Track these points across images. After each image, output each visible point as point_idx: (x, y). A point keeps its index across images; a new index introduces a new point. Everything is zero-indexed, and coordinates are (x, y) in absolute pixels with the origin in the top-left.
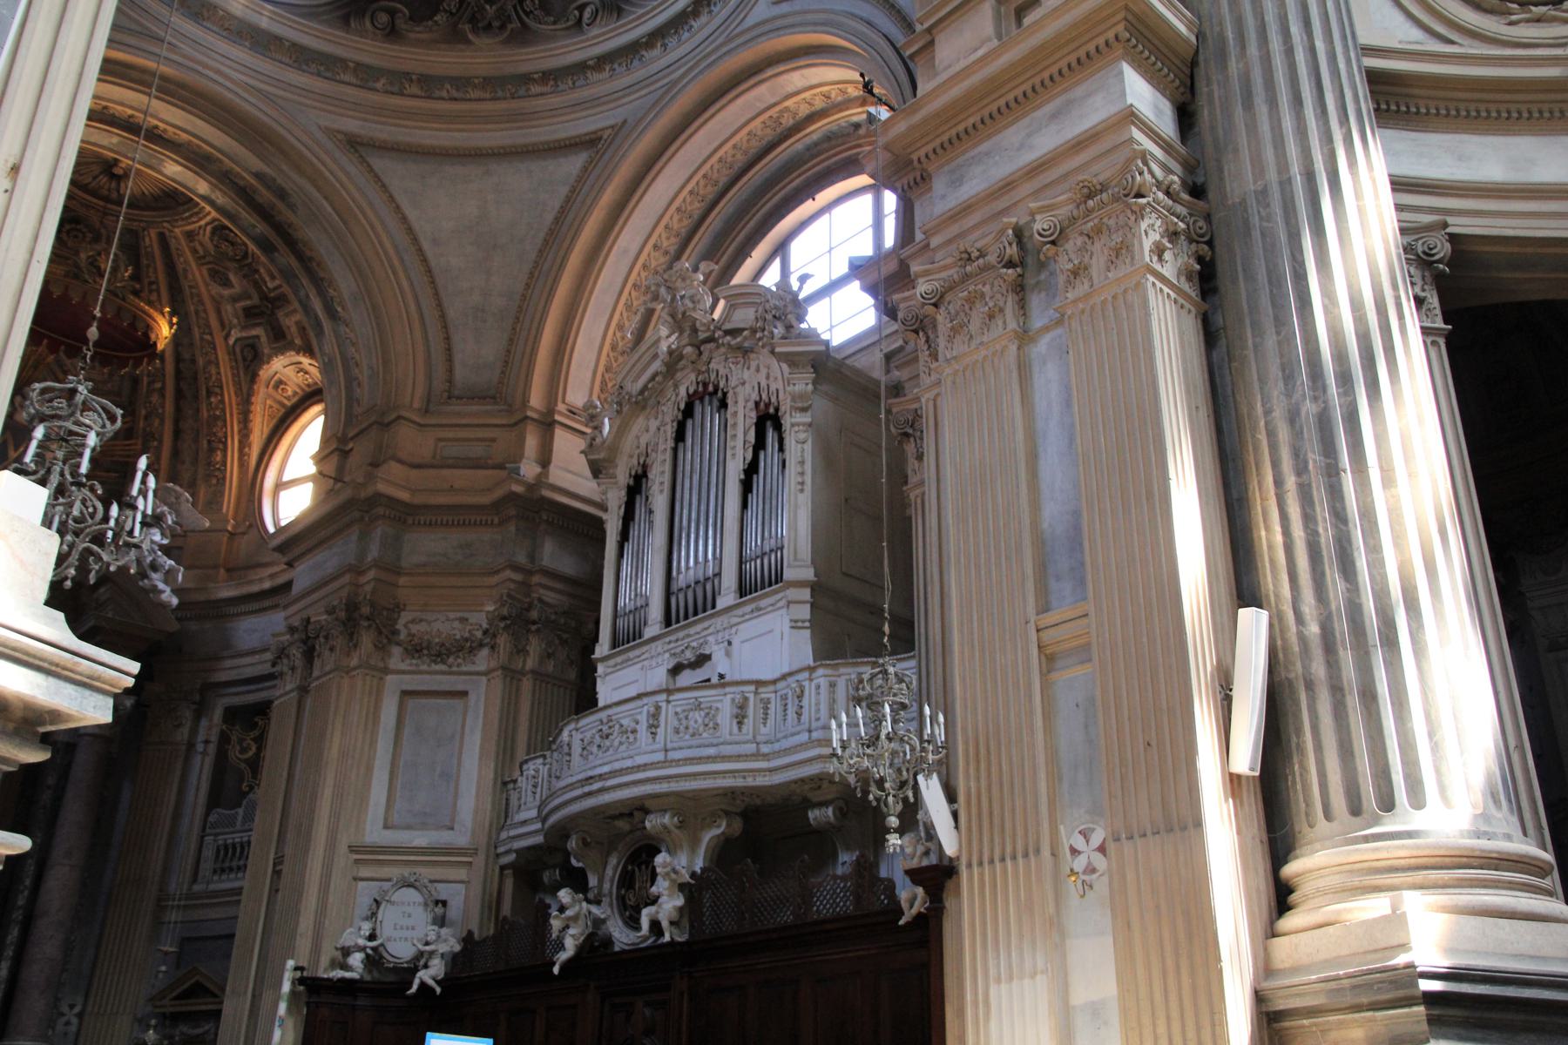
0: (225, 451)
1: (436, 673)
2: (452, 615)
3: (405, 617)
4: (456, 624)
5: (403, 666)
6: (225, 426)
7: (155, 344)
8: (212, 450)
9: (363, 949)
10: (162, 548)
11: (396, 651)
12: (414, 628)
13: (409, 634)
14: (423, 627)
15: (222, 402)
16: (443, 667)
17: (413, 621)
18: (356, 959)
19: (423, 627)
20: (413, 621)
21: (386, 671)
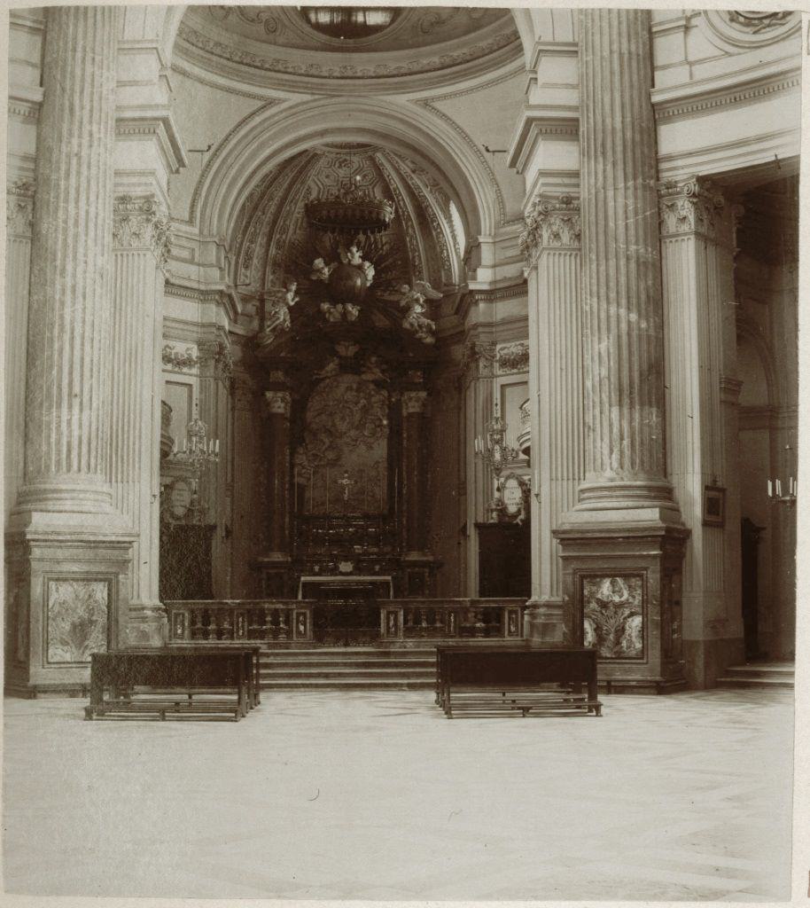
0: (447, 250)
1: (513, 374)
2: (518, 343)
3: (498, 347)
4: (520, 347)
5: (500, 372)
6: (444, 236)
7: (384, 220)
8: (442, 252)
9: (496, 510)
10: (422, 314)
11: (497, 365)
12: (502, 352)
13: (501, 356)
14: (506, 351)
15: (439, 224)
16: (515, 371)
17: (502, 349)
18: (495, 514)
19: (506, 351)
20: (502, 349)
21: (494, 376)
